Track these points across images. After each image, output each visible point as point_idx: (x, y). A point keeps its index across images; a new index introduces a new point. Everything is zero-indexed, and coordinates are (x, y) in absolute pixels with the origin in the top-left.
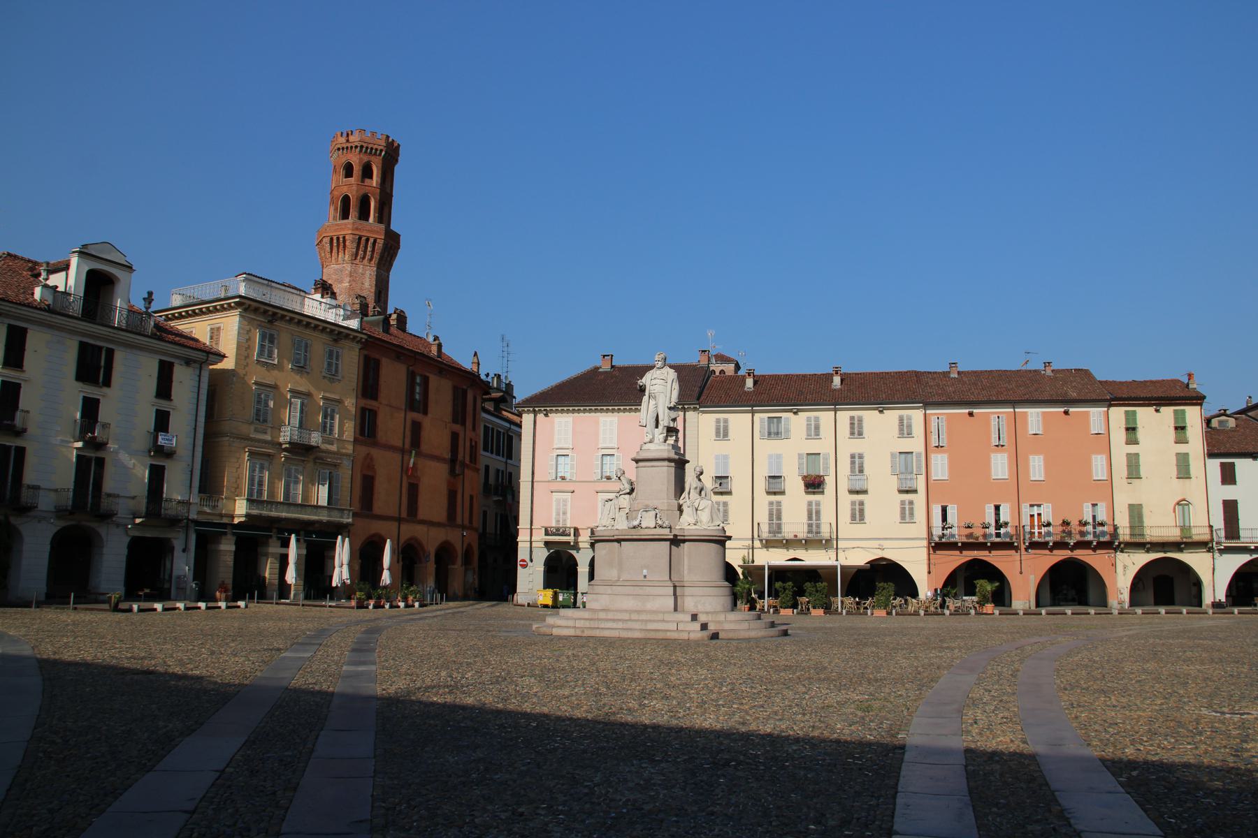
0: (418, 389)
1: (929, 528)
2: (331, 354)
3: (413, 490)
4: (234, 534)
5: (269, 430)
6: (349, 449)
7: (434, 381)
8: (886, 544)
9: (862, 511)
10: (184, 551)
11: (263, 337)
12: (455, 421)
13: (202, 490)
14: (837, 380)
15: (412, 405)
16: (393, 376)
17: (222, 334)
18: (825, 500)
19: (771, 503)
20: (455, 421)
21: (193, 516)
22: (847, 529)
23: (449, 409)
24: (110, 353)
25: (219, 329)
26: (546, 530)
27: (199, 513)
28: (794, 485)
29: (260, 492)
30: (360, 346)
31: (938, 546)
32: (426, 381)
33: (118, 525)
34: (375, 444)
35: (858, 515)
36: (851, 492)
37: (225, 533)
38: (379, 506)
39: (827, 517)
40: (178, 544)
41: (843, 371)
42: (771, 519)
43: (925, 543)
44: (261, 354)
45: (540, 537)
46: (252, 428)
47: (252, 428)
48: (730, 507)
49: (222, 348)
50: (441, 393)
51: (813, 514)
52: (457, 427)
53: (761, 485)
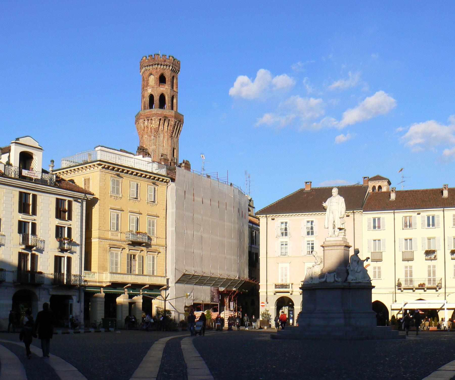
5: (119, 234)
10: (78, 302)
11: (113, 183)
14: (446, 194)
17: (91, 182)
18: (439, 264)
19: (406, 267)
24: (35, 197)
25: (89, 179)
26: (276, 285)
28: (419, 255)
29: (116, 268)
33: (44, 289)
39: (439, 275)
40: (75, 299)
41: (449, 187)
42: (406, 276)
44: (113, 192)
45: (272, 289)
46: (110, 233)
47: (110, 233)
48: (382, 270)
49: (91, 190)
51: (431, 272)
53: (399, 257)
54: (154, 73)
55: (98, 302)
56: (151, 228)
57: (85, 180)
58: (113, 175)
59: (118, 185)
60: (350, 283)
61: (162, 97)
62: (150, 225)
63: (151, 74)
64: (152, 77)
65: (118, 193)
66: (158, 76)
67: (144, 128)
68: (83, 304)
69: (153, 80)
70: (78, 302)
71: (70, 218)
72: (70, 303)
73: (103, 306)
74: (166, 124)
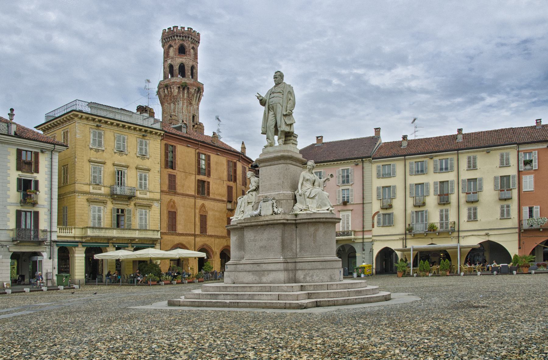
0: (203, 162)
1: (520, 221)
2: (141, 144)
3: (203, 219)
4: (83, 246)
6: (157, 196)
7: (214, 158)
8: (491, 233)
9: (475, 214)
11: (94, 135)
12: (229, 180)
13: (59, 224)
15: (199, 171)
16: (185, 154)
20: (229, 180)
21: (54, 238)
22: (465, 225)
23: (226, 173)
27: (58, 237)
29: (99, 223)
30: (160, 138)
31: (524, 233)
32: (208, 158)
34: (175, 193)
35: (473, 217)
36: (468, 202)
37: (77, 246)
38: (180, 228)
43: (517, 230)
44: (94, 144)
47: (91, 187)
50: (219, 164)
52: (231, 184)
54: (173, 44)
55: (76, 258)
56: (143, 182)
57: (64, 133)
58: (93, 127)
59: (100, 137)
60: (296, 215)
61: (182, 68)
62: (141, 179)
63: (171, 46)
64: (172, 49)
65: (100, 144)
66: (176, 47)
67: (165, 96)
68: (56, 260)
69: (172, 52)
70: (50, 258)
71: (37, 171)
72: (39, 259)
73: (84, 261)
74: (186, 92)
